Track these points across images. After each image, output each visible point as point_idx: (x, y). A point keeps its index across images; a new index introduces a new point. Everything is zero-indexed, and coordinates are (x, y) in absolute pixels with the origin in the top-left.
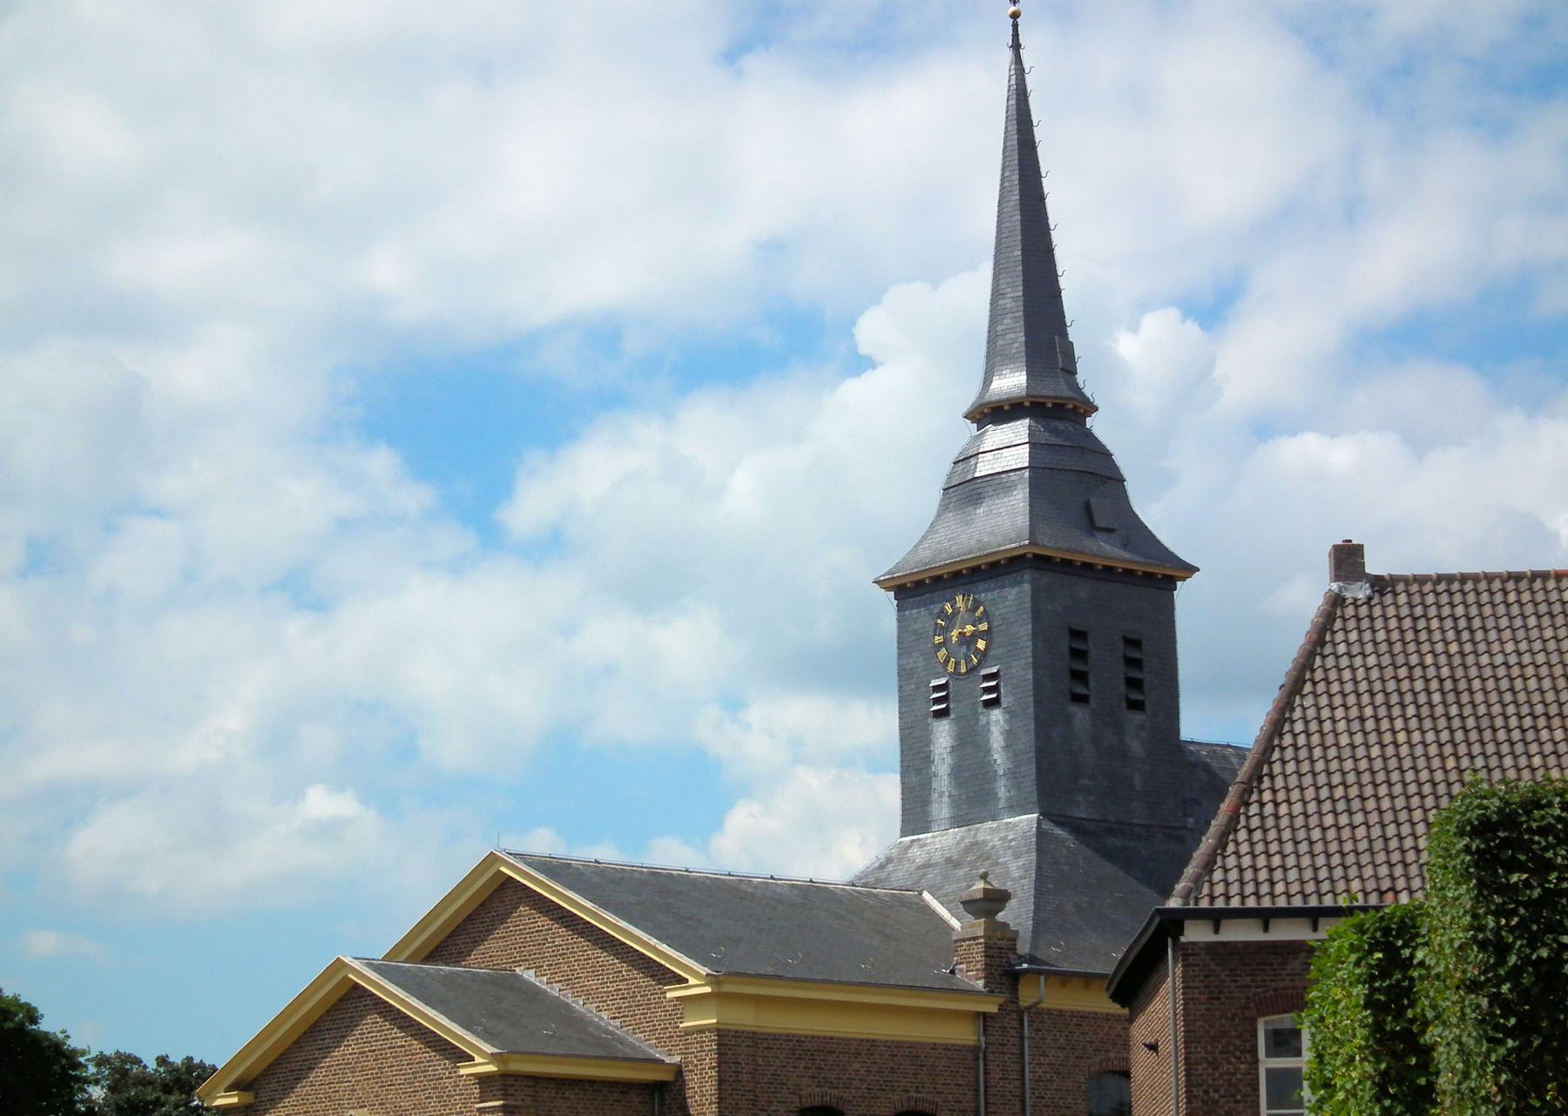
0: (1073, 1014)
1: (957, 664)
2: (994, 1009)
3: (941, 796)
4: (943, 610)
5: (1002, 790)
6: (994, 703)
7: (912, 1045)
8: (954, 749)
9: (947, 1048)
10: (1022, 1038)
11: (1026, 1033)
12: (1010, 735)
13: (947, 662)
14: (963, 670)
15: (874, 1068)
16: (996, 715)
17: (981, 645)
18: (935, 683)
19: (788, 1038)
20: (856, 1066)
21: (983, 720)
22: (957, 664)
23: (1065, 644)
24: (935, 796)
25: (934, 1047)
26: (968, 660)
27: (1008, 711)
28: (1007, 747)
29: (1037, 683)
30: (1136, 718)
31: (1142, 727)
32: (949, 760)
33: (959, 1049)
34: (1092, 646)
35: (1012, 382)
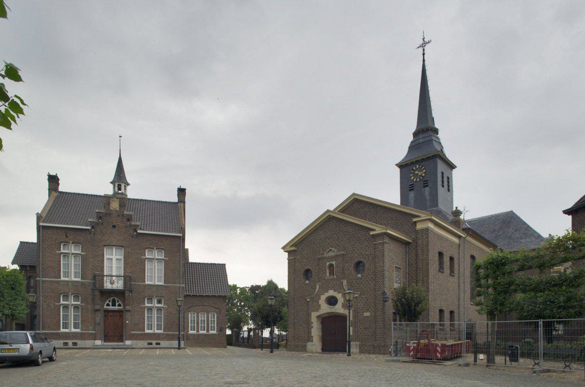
1: (417, 179)
4: (413, 169)
5: (428, 203)
6: (427, 186)
14: (418, 180)
16: (427, 189)
22: (417, 179)
32: (413, 199)
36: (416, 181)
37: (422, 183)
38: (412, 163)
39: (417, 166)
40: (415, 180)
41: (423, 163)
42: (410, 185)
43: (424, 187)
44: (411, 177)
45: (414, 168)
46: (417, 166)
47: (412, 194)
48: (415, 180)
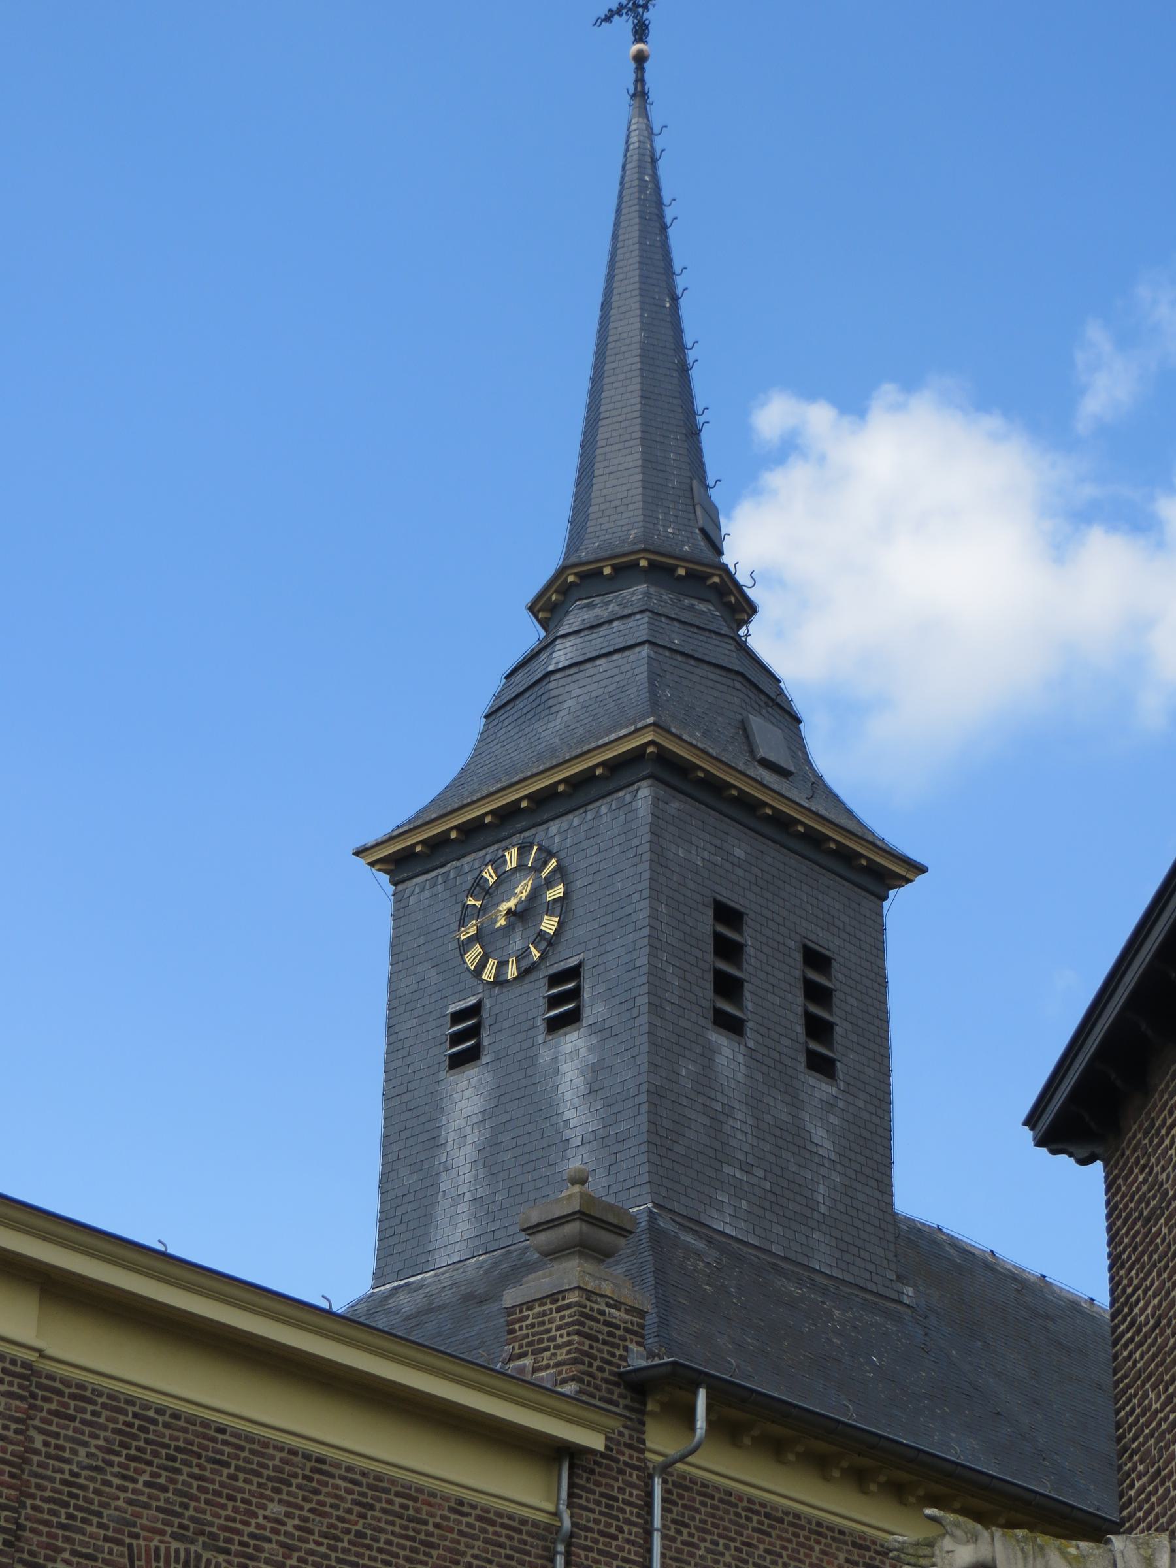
0: (754, 1507)
1: (502, 964)
2: (596, 1442)
3: (454, 1204)
4: (479, 881)
7: (409, 1493)
8: (485, 1116)
9: (486, 1517)
10: (648, 1533)
11: (657, 1523)
12: (596, 1073)
13: (482, 965)
14: (512, 972)
15: (318, 1525)
16: (573, 1041)
17: (549, 924)
18: (454, 1008)
19: (116, 1403)
20: (274, 1509)
21: (545, 1055)
22: (502, 964)
23: (706, 923)
24: (444, 1204)
25: (459, 1507)
26: (524, 954)
27: (599, 1029)
28: (592, 1090)
29: (654, 972)
30: (823, 1088)
31: (829, 1106)
32: (475, 1136)
33: (514, 1525)
34: (748, 937)
35: (623, 523)
36: (500, 981)
37: (541, 991)
38: (472, 832)
39: (512, 858)
40: (488, 975)
41: (554, 828)
42: (457, 1017)
43: (555, 1025)
44: (464, 946)
45: (490, 875)
46: (512, 858)
47: (467, 1095)
48: (488, 975)
